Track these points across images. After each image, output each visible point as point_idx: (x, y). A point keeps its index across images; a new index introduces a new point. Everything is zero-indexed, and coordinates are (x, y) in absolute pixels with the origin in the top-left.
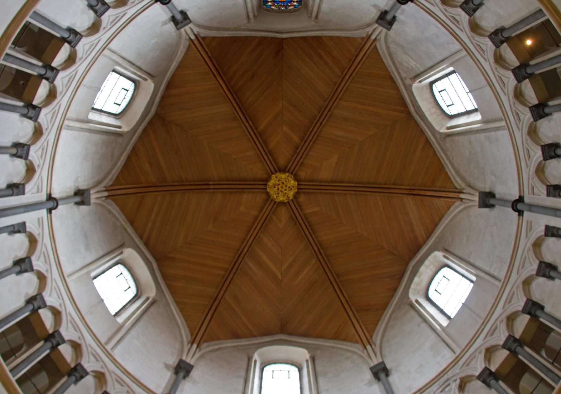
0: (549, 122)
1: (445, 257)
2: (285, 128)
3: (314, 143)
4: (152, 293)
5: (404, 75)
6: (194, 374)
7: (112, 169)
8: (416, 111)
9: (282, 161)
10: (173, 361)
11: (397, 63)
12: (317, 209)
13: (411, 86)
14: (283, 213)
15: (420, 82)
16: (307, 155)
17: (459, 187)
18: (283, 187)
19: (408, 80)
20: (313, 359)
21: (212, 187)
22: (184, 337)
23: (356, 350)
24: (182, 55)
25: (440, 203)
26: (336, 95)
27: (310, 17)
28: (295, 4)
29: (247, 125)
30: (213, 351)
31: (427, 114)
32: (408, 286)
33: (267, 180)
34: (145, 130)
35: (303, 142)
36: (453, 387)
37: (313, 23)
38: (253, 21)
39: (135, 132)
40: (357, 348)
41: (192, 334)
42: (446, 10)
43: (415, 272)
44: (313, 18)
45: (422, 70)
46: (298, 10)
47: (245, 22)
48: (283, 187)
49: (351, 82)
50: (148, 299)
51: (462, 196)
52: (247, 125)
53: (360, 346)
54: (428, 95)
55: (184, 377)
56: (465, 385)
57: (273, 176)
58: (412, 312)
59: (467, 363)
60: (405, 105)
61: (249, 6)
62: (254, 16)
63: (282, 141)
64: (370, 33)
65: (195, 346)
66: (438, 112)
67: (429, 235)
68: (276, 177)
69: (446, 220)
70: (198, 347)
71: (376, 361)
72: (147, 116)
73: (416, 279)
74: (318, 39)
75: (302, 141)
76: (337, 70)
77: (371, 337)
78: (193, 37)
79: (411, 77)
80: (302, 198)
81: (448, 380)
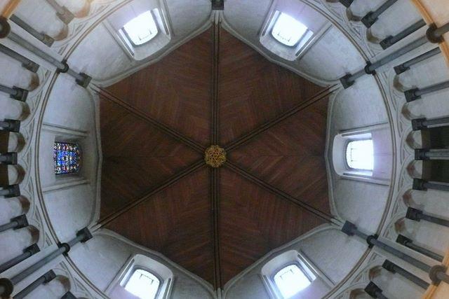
1: (263, 35)
4: (295, 253)
5: (128, 67)
6: (353, 220)
7: (203, 287)
10: (344, 236)
12: (231, 130)
14: (236, 155)
15: (133, 54)
17: (211, 25)
18: (215, 156)
20: (342, 131)
21: (216, 209)
22: (326, 228)
23: (334, 99)
27: (85, 137)
30: (337, 207)
31: (158, 49)
32: (286, 61)
33: (209, 166)
36: (356, 25)
37: (90, 135)
38: (88, 180)
39: (174, 268)
40: (332, 98)
41: (325, 223)
43: (275, 56)
44: (86, 135)
45: (123, 53)
46: (80, 146)
47: (89, 186)
48: (215, 156)
50: (299, 256)
51: (217, 23)
53: (331, 96)
54: (144, 49)
55: (356, 228)
56: (355, 17)
57: (207, 163)
58: (304, 58)
59: (338, 15)
61: (77, 183)
65: (332, 220)
67: (249, 47)
69: (236, 34)
70: (334, 218)
71: (340, 85)
72: (162, 259)
73: (281, 56)
77: (324, 88)
78: (100, 226)
80: (224, 142)
81: (351, 30)
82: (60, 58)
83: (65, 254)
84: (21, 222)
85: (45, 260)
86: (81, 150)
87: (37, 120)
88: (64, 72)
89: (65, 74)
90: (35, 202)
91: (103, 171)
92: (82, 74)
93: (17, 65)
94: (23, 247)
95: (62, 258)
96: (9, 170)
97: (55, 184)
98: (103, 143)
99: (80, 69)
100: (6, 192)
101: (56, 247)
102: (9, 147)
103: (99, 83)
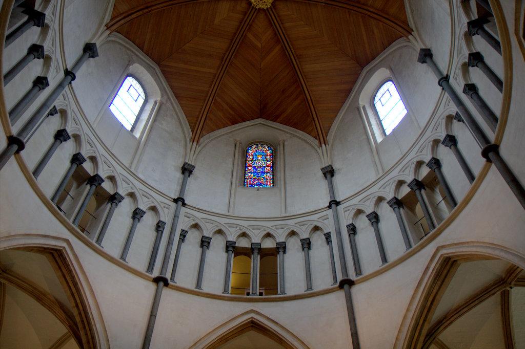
0: (70, 154)
2: (259, 45)
3: (235, 34)
5: (169, 104)
8: (154, 69)
9: (262, 16)
11: (175, 116)
13: (162, 96)
15: (156, 103)
16: (241, 23)
19: (165, 102)
24: (335, 122)
25: (124, 8)
26: (219, 80)
28: (251, 152)
29: (290, 53)
31: (145, 72)
34: (373, 58)
35: (244, 34)
37: (238, 139)
42: (153, 202)
44: (238, 145)
49: (208, 91)
52: (290, 53)
60: (163, 72)
61: (282, 156)
62: (280, 144)
63: (261, 35)
64: (198, 146)
66: (137, 75)
68: (267, 5)
74: (234, 122)
75: (246, 34)
76: (219, 100)
79: (163, 107)
82: (173, 205)
83: (338, 204)
84: (306, 245)
85: (339, 233)
86: (252, 143)
87: (227, 221)
88: (184, 201)
89: (185, 198)
90: (292, 224)
91: (275, 120)
92: (183, 173)
93: (184, 246)
94: (325, 243)
95: (340, 208)
96: (265, 247)
97: (280, 190)
98: (244, 120)
99: (178, 175)
100: (281, 253)
101: (331, 210)
102: (247, 246)
103: (188, 143)
